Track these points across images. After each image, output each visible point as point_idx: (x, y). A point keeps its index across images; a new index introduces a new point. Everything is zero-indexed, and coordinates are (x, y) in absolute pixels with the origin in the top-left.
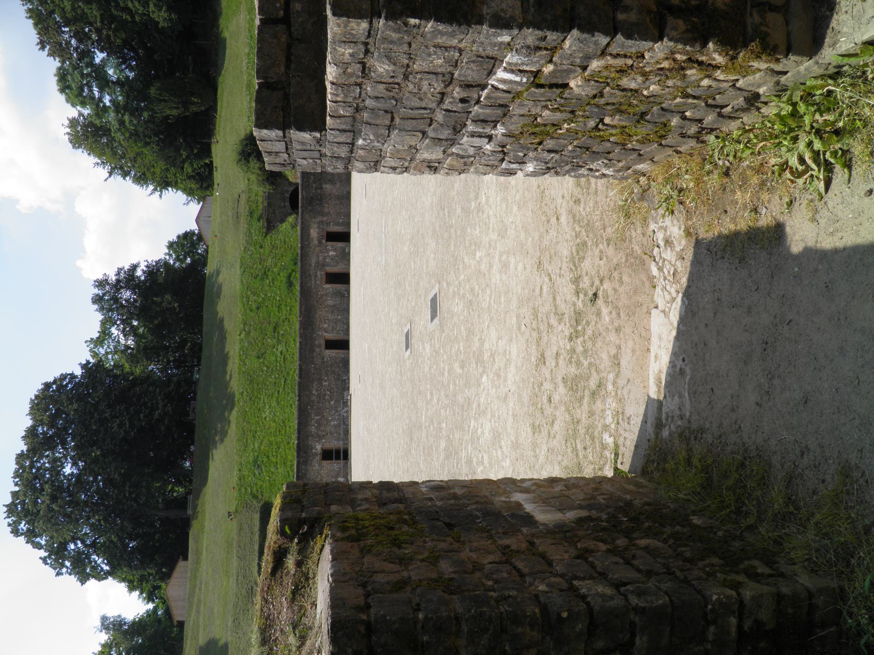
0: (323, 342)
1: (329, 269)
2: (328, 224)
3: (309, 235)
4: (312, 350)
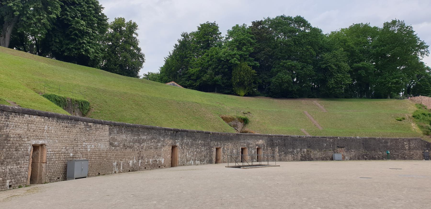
0: (218, 147)
1: (247, 150)
2: (264, 149)
3: (260, 139)
4: (216, 140)
